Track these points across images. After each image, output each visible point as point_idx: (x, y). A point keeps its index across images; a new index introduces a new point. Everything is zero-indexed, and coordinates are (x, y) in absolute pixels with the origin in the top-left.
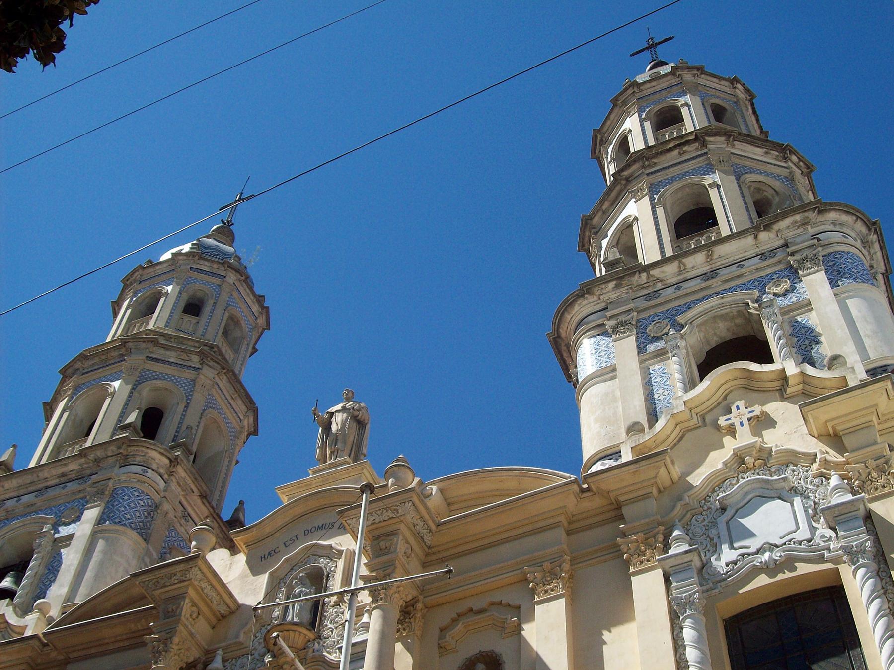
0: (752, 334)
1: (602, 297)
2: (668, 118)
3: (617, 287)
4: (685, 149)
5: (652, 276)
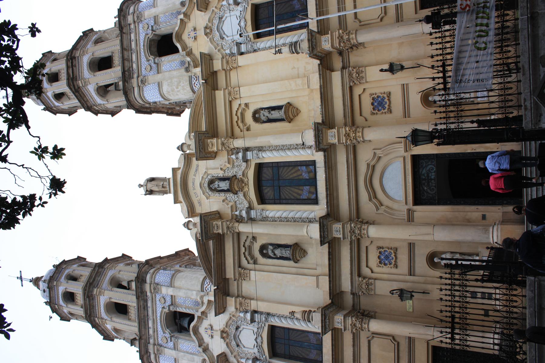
3: (127, 82)
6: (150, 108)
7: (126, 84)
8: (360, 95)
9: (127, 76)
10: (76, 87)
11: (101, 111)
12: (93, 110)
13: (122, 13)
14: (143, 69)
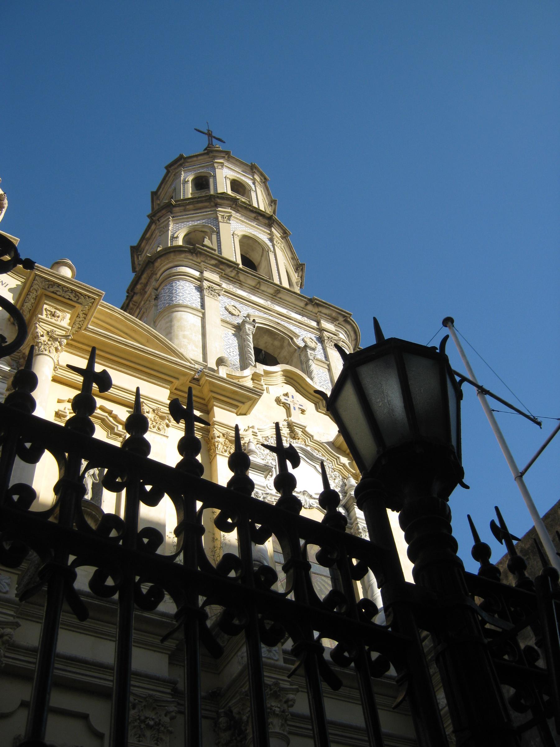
0: (276, 356)
1: (202, 263)
2: (201, 183)
4: (260, 218)
5: (238, 277)
6: (143, 291)
7: (213, 262)
8: (85, 717)
9: (228, 270)
10: (219, 201)
11: (153, 227)
12: (164, 212)
13: (341, 319)
14: (233, 303)
